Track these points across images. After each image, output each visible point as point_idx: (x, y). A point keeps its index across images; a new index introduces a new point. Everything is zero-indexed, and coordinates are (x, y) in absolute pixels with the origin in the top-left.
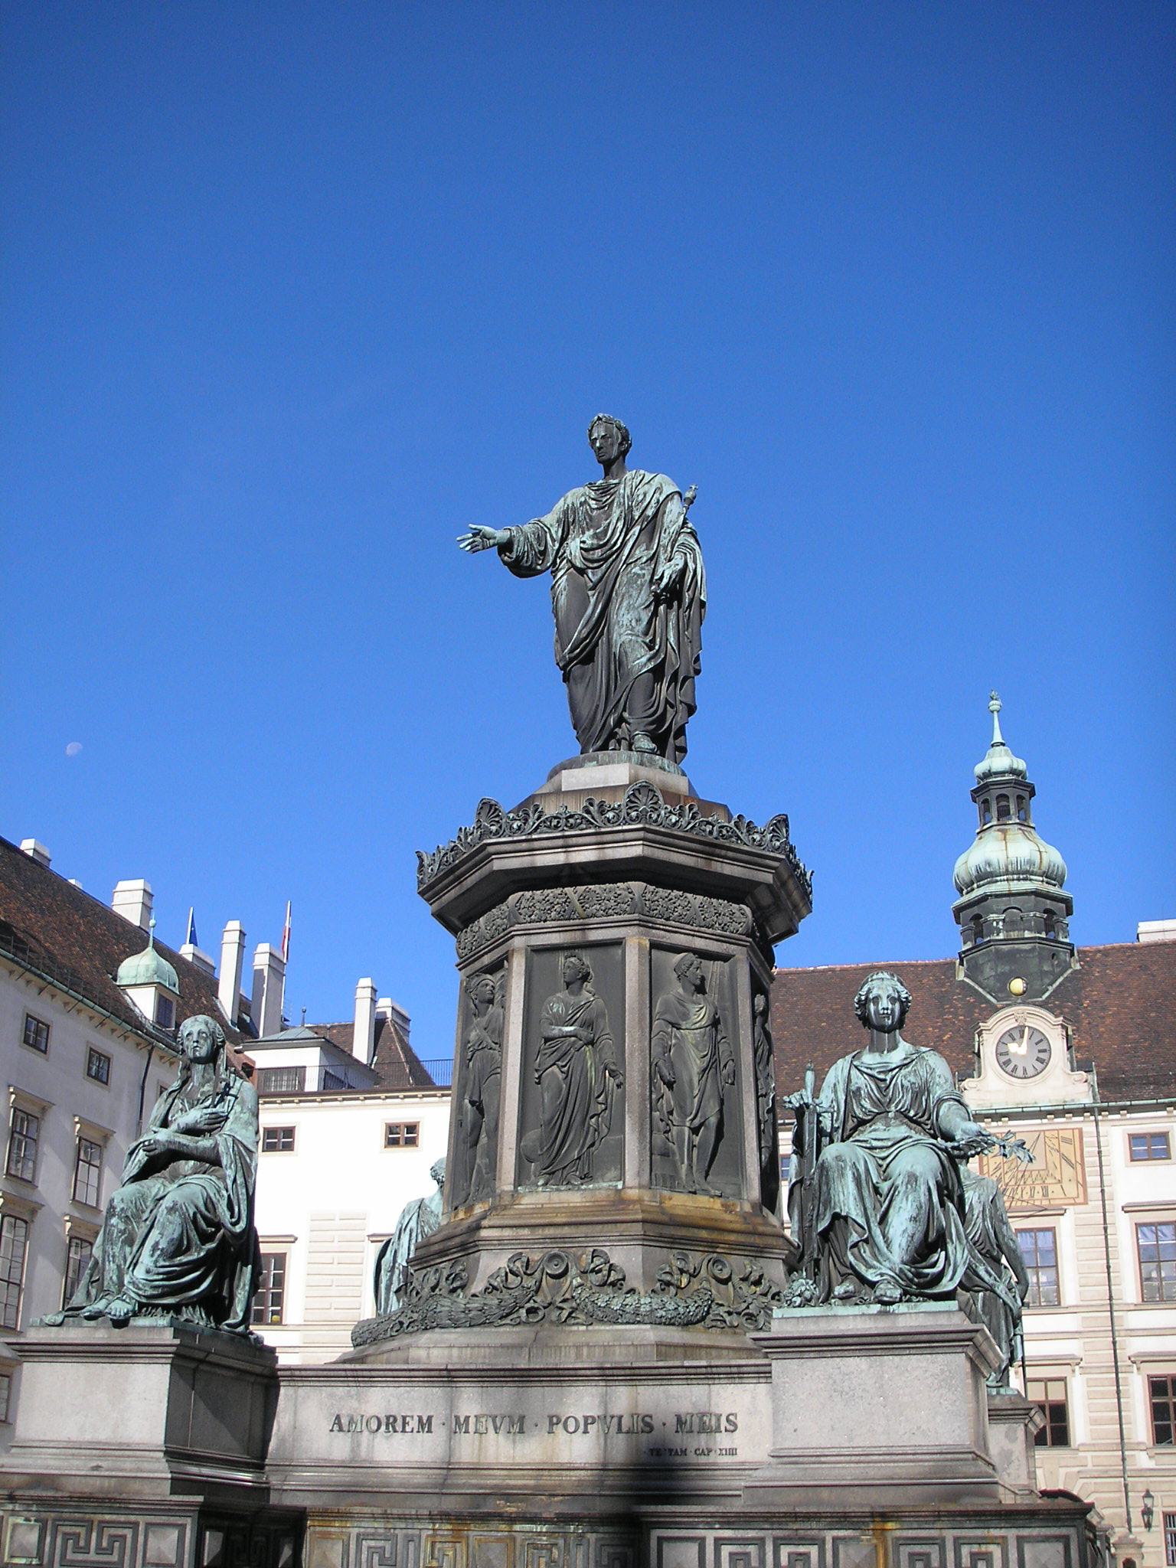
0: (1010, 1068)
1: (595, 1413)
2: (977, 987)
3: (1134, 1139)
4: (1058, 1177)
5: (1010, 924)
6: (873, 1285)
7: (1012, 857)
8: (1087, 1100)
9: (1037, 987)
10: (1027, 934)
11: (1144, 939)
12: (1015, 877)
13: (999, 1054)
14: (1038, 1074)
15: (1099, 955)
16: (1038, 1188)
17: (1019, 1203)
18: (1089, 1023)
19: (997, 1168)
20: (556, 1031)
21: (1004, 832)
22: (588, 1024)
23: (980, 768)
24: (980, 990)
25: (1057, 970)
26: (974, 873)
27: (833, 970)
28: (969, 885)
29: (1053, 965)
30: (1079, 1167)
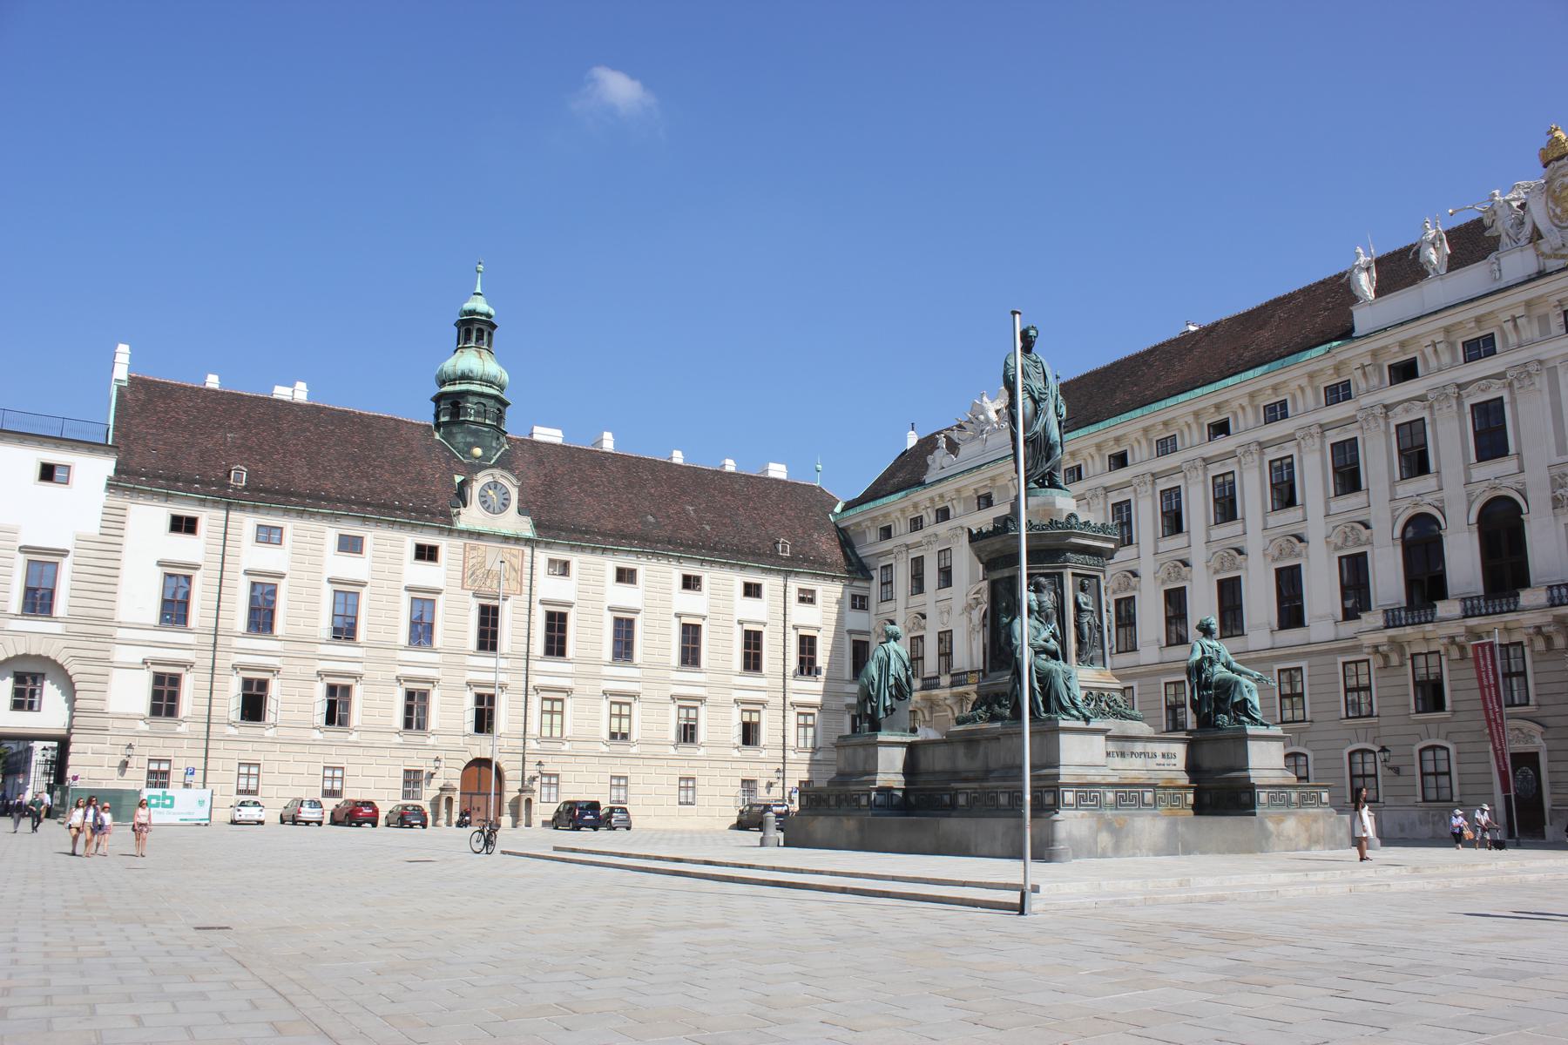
0: (486, 505)
1: (1142, 751)
3: (552, 562)
4: (507, 577)
5: (478, 413)
6: (1256, 720)
10: (487, 422)
19: (473, 565)
21: (479, 353)
23: (468, 306)
26: (459, 373)
27: (354, 412)
28: (453, 381)
29: (497, 444)
30: (519, 573)
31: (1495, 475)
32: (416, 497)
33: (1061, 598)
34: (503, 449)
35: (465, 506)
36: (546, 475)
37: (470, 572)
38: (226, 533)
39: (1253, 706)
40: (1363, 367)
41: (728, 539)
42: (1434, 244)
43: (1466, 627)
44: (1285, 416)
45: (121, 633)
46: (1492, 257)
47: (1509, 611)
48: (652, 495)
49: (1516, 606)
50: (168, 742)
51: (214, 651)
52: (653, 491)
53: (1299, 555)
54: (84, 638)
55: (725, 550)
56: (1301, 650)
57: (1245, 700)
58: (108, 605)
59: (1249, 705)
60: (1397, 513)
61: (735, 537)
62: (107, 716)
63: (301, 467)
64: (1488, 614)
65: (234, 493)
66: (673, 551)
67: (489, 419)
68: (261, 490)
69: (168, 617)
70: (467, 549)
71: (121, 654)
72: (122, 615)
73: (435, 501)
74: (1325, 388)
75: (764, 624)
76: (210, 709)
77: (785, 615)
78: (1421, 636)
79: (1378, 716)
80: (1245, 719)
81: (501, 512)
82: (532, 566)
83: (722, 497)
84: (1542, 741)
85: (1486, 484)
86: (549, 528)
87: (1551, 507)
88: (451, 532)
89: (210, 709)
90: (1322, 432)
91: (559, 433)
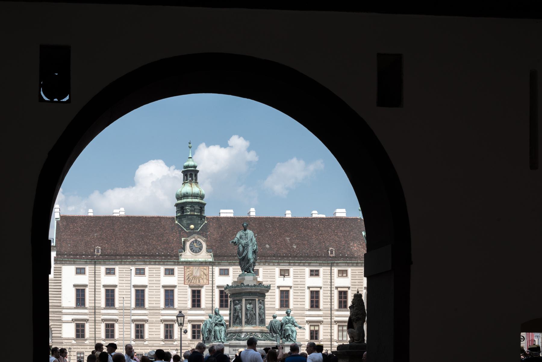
0: (193, 250)
2: (181, 226)
4: (203, 278)
5: (191, 211)
7: (194, 191)
8: (211, 260)
9: (197, 227)
10: (196, 214)
11: (222, 215)
12: (194, 197)
13: (190, 247)
14: (199, 252)
15: (211, 219)
16: (198, 280)
17: (193, 284)
18: (210, 239)
19: (188, 275)
20: (249, 309)
21: (191, 184)
22: (252, 308)
23: (186, 164)
24: (182, 227)
25: (202, 223)
27: (143, 217)
29: (201, 222)
32: (165, 250)
33: (241, 306)
34: (204, 223)
35: (184, 251)
36: (222, 233)
37: (187, 278)
38: (95, 272)
39: (292, 336)
41: (304, 251)
45: (64, 311)
48: (270, 235)
50: (82, 347)
51: (95, 315)
52: (271, 233)
54: (53, 313)
55: (301, 257)
57: (289, 335)
58: (59, 301)
59: (291, 336)
61: (308, 249)
62: (62, 339)
63: (121, 244)
65: (97, 257)
66: (275, 260)
67: (196, 212)
68: (106, 255)
69: (78, 304)
70: (186, 269)
71: (65, 318)
72: (64, 304)
73: (173, 251)
75: (321, 288)
76: (95, 335)
77: (331, 282)
80: (289, 340)
81: (199, 252)
82: (213, 273)
83: (306, 231)
86: (220, 256)
88: (179, 263)
89: (95, 335)
91: (232, 211)
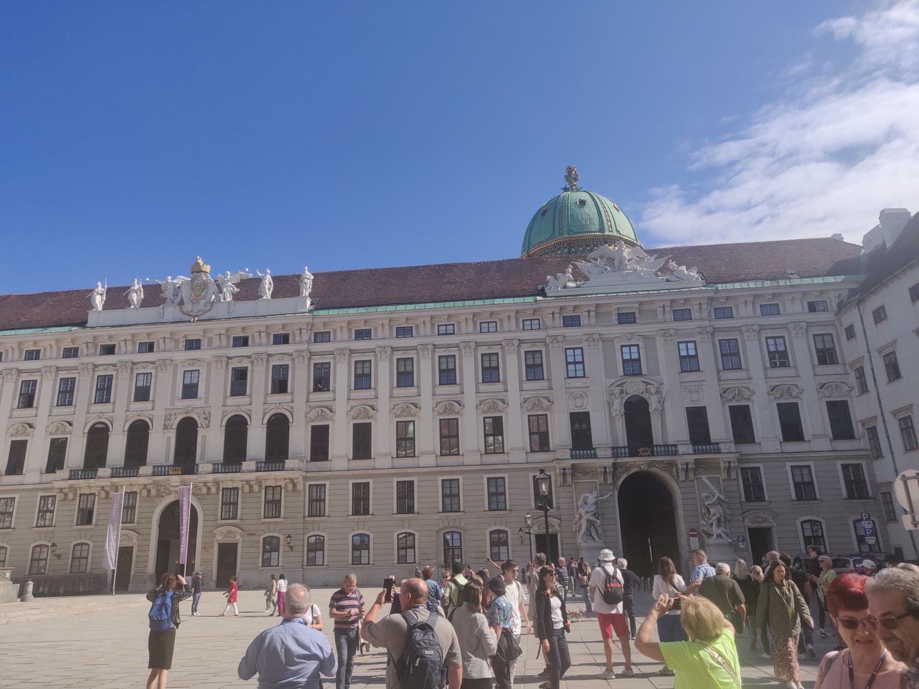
31: (140, 410)
40: (87, 343)
42: (136, 293)
43: (111, 482)
44: (37, 358)
46: (161, 307)
47: (133, 476)
49: (137, 474)
53: (28, 435)
56: (17, 487)
60: (88, 420)
64: (123, 477)
74: (64, 349)
78: (87, 485)
79: (55, 526)
84: (136, 541)
85: (136, 412)
87: (162, 428)
90: (57, 371)
